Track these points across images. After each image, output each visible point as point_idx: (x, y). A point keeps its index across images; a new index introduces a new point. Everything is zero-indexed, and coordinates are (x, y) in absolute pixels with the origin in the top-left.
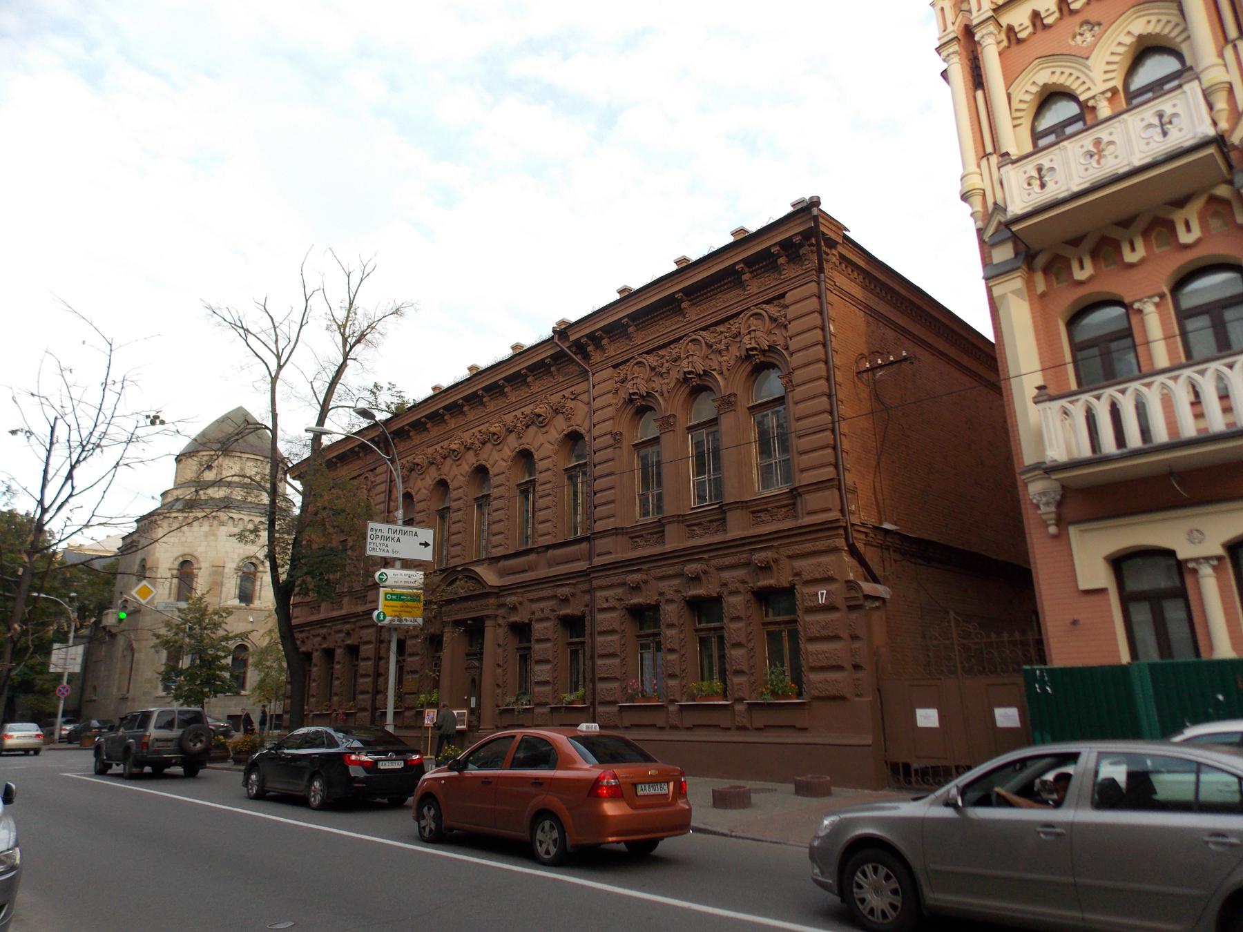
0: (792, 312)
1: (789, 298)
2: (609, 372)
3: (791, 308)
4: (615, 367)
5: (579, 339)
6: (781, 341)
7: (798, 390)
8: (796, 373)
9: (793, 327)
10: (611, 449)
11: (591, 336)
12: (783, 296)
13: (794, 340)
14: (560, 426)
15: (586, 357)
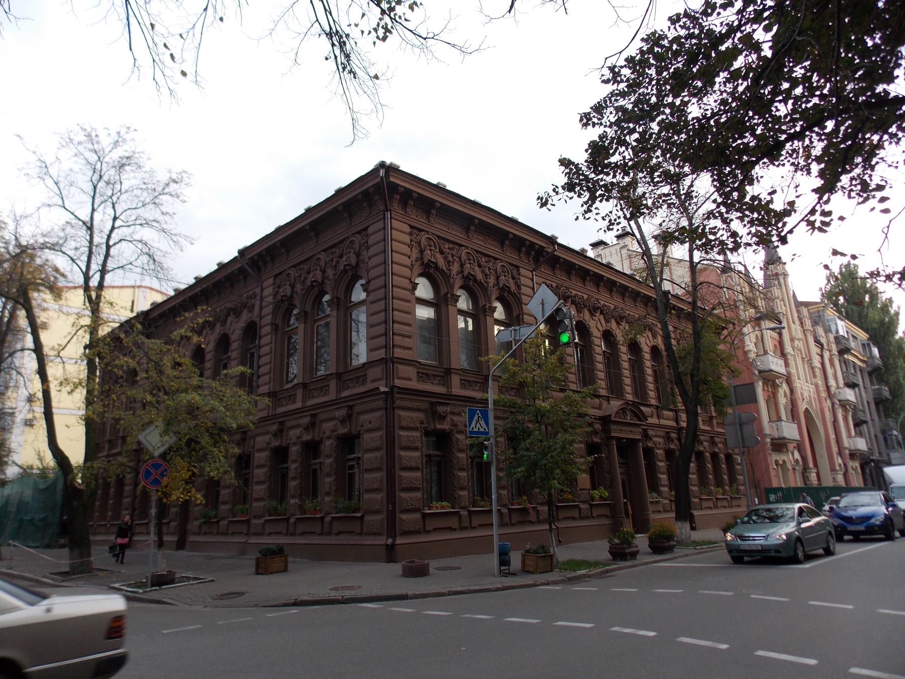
0: (371, 240)
1: (371, 230)
2: (271, 281)
3: (373, 237)
4: (276, 276)
5: (252, 257)
6: (366, 260)
7: (372, 294)
8: (372, 283)
9: (372, 251)
10: (269, 336)
11: (259, 254)
12: (366, 229)
13: (372, 260)
14: (245, 316)
15: (259, 269)
